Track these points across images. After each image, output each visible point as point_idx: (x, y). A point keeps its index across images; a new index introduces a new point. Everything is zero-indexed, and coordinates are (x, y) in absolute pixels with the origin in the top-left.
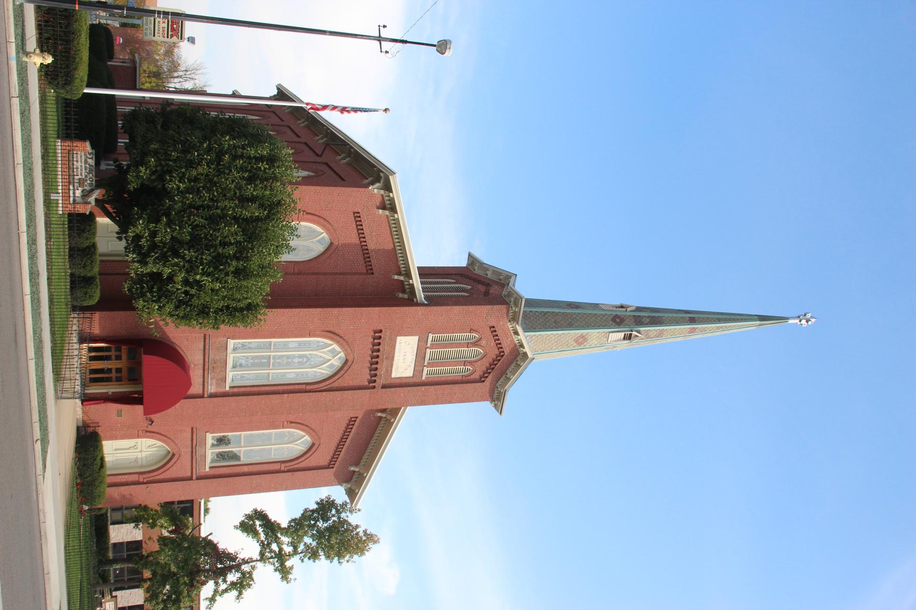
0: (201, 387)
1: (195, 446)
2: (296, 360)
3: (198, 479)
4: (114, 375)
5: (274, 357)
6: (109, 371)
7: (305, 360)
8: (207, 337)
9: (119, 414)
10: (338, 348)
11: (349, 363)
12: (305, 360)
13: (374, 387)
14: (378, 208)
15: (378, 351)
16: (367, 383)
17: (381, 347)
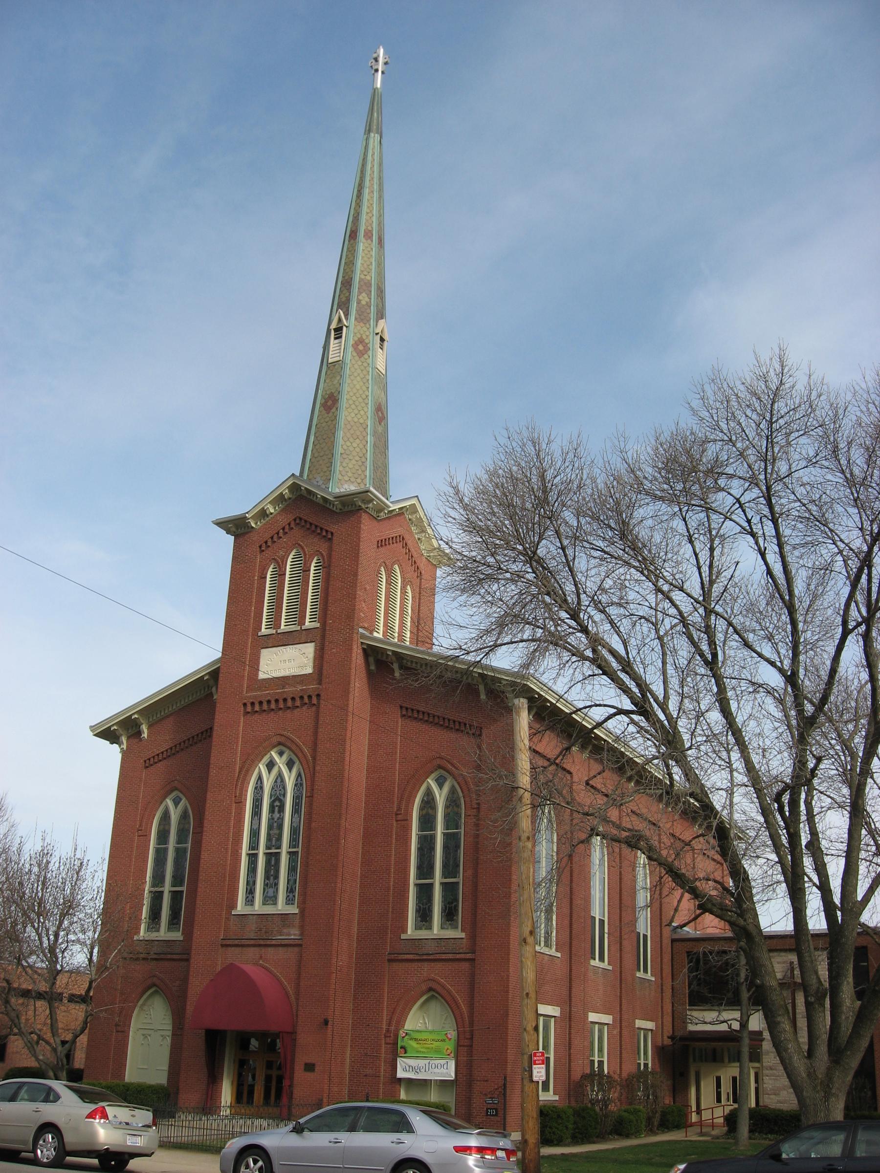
0: (290, 949)
1: (420, 954)
2: (276, 815)
3: (474, 952)
4: (274, 1073)
5: (268, 848)
6: (268, 1079)
7: (277, 803)
8: (225, 942)
9: (310, 1067)
10: (266, 759)
11: (282, 739)
12: (277, 803)
13: (318, 695)
14: (141, 740)
15: (286, 697)
16: (314, 708)
17: (264, 700)
